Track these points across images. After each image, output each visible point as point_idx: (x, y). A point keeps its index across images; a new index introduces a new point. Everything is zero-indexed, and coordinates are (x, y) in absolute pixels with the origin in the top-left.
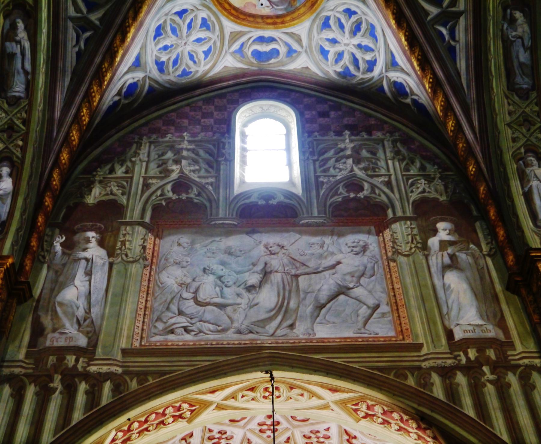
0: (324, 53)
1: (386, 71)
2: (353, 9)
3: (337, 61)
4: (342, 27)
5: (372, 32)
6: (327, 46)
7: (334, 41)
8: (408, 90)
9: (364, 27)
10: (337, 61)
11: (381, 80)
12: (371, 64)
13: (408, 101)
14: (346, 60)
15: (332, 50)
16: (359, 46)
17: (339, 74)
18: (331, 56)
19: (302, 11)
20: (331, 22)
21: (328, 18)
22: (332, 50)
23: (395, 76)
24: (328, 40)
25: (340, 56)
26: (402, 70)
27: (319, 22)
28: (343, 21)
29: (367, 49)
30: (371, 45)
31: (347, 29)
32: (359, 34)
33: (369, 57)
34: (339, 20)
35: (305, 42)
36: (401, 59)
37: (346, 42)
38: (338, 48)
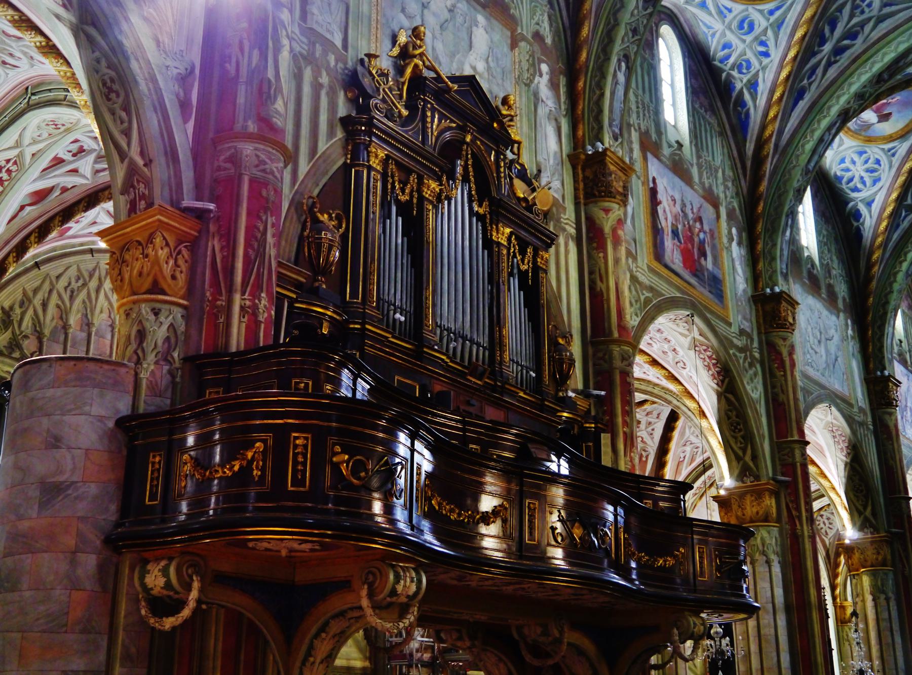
0: (843, 161)
1: (860, 201)
2: (882, 163)
3: (842, 170)
4: (866, 162)
5: (876, 181)
6: (848, 160)
7: (854, 163)
8: (861, 220)
9: (876, 174)
10: (842, 170)
11: (852, 200)
12: (856, 189)
13: (855, 224)
14: (848, 175)
15: (848, 164)
16: (862, 178)
17: (836, 175)
18: (843, 166)
19: (860, 137)
20: (865, 155)
21: (865, 152)
22: (848, 164)
23: (862, 208)
24: (852, 159)
25: (848, 170)
26: (870, 212)
27: (860, 149)
28: (870, 161)
29: (864, 183)
30: (868, 184)
31: (866, 166)
32: (869, 174)
33: (860, 186)
34: (869, 159)
35: (841, 148)
36: (876, 207)
37: (859, 169)
38: (851, 167)
